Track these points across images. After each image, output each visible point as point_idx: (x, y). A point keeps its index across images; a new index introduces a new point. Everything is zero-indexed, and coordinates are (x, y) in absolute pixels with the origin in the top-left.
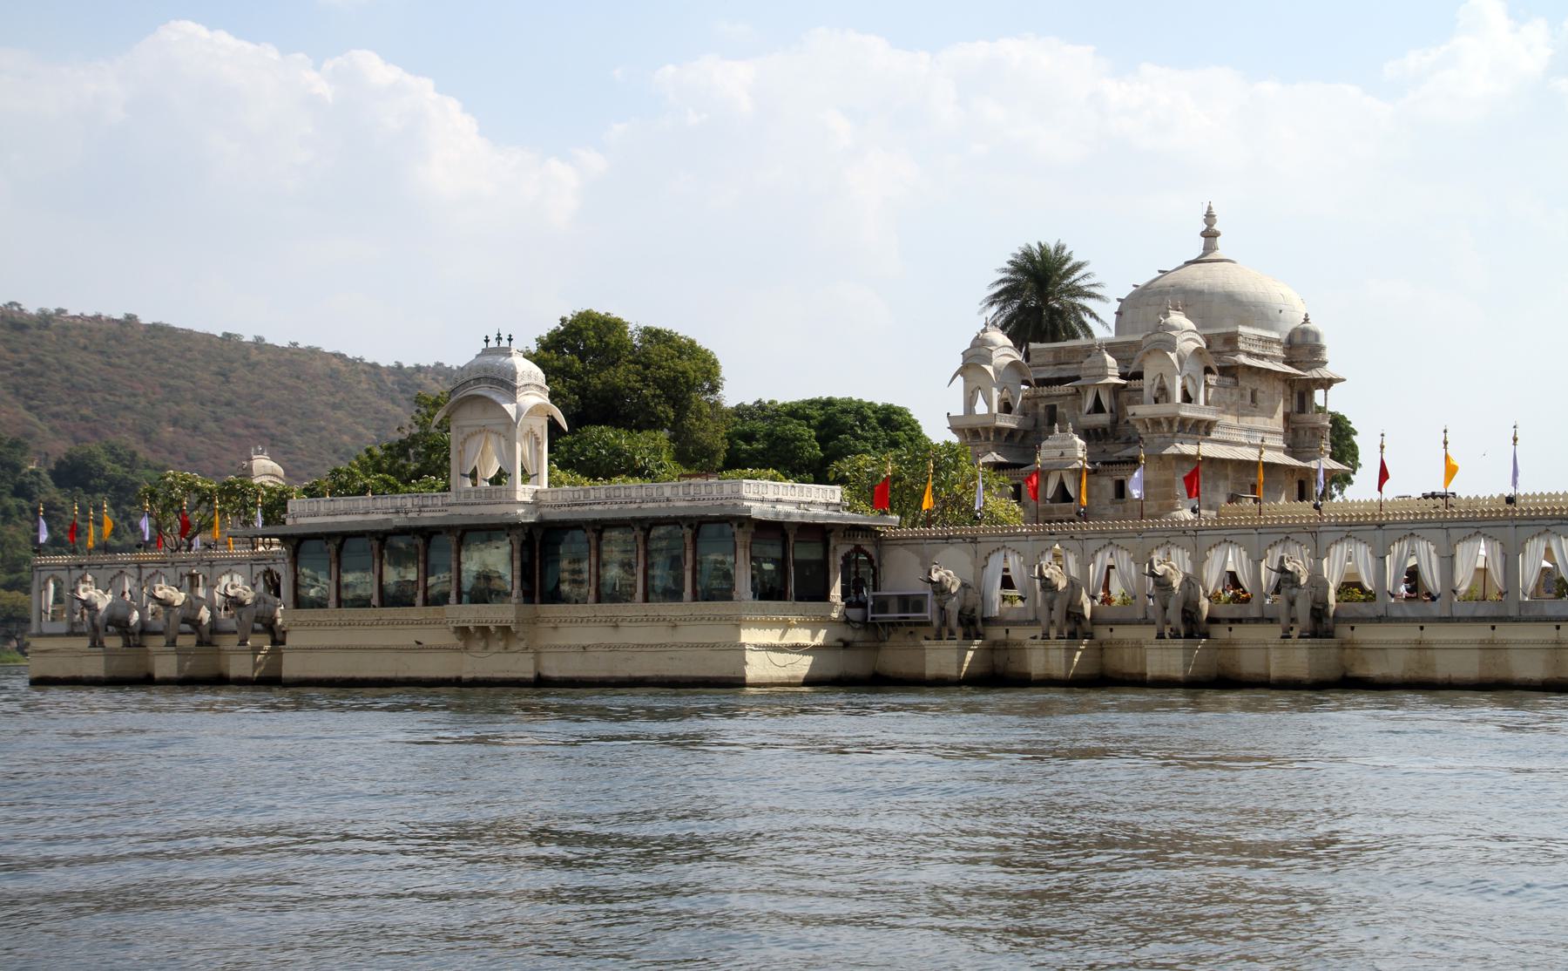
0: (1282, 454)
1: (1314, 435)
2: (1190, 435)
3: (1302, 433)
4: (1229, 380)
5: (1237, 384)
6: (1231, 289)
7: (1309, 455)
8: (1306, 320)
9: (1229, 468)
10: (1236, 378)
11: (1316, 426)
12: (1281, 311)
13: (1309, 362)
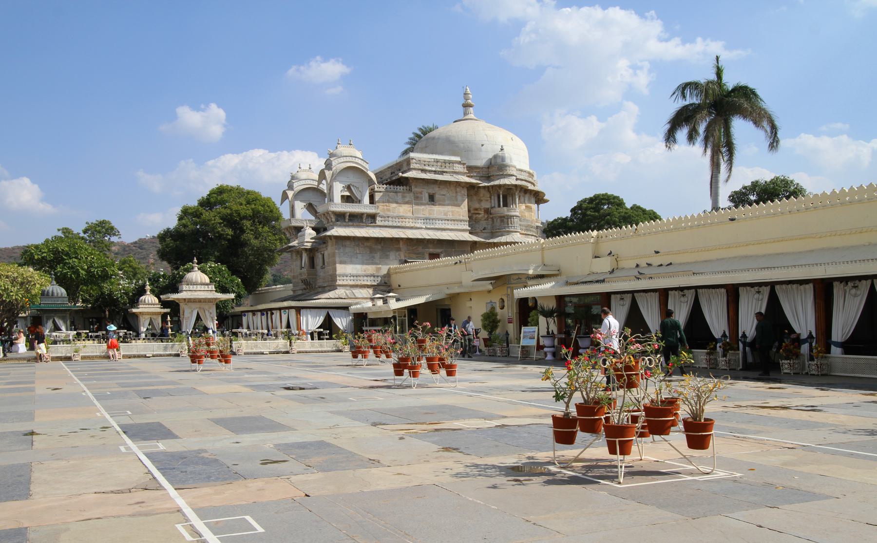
0: (467, 233)
1: (502, 221)
2: (350, 223)
3: (495, 220)
4: (400, 188)
5: (410, 190)
6: (450, 134)
7: (500, 234)
8: (502, 150)
9: (401, 243)
10: (410, 187)
11: (502, 215)
12: (482, 145)
13: (498, 175)
